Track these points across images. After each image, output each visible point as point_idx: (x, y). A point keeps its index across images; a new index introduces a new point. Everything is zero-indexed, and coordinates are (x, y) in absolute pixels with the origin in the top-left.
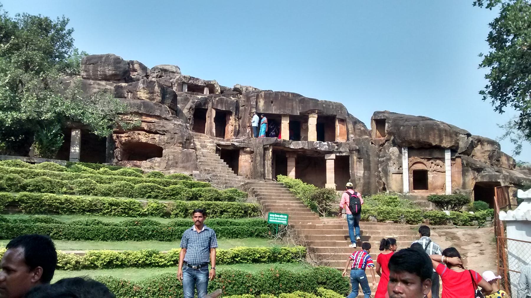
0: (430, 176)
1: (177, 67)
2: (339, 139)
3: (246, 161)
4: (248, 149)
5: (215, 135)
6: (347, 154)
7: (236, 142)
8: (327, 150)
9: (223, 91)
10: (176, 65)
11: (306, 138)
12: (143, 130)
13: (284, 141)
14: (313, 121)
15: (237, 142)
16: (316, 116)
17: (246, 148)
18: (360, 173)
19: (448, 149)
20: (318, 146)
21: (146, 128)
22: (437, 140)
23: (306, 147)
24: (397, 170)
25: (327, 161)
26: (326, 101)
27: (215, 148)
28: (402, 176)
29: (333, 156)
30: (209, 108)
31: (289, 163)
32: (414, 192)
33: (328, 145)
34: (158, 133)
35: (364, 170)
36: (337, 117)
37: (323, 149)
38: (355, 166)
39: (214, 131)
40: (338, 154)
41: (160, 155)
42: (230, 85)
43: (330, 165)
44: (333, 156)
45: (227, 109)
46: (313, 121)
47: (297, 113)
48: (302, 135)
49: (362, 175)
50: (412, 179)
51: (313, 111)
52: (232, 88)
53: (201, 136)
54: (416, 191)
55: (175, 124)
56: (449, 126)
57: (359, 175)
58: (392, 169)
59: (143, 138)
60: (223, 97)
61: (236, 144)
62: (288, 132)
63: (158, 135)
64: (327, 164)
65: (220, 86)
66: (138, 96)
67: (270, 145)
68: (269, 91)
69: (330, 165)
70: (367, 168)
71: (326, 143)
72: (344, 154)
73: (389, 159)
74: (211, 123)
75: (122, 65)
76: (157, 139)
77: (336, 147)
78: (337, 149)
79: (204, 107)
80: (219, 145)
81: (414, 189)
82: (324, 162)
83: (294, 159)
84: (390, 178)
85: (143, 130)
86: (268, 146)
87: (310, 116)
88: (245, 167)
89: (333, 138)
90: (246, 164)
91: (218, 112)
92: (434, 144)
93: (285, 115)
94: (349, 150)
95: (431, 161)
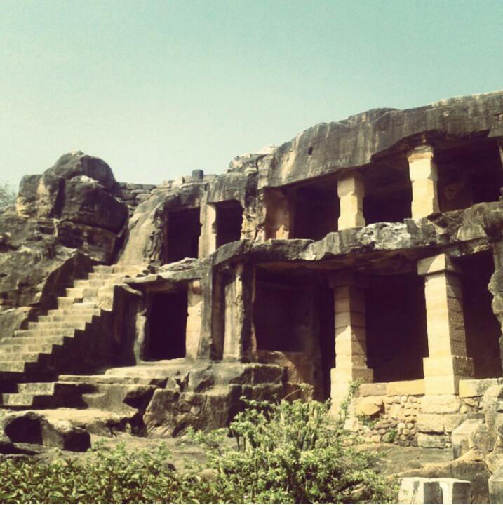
4: (196, 284)
6: (484, 247)
8: (409, 245)
15: (172, 269)
20: (373, 238)
23: (336, 250)
29: (439, 262)
30: (203, 205)
37: (392, 245)
40: (457, 253)
51: (412, 143)
74: (206, 237)
77: (440, 231)
78: (446, 236)
79: (190, 207)
91: (219, 207)
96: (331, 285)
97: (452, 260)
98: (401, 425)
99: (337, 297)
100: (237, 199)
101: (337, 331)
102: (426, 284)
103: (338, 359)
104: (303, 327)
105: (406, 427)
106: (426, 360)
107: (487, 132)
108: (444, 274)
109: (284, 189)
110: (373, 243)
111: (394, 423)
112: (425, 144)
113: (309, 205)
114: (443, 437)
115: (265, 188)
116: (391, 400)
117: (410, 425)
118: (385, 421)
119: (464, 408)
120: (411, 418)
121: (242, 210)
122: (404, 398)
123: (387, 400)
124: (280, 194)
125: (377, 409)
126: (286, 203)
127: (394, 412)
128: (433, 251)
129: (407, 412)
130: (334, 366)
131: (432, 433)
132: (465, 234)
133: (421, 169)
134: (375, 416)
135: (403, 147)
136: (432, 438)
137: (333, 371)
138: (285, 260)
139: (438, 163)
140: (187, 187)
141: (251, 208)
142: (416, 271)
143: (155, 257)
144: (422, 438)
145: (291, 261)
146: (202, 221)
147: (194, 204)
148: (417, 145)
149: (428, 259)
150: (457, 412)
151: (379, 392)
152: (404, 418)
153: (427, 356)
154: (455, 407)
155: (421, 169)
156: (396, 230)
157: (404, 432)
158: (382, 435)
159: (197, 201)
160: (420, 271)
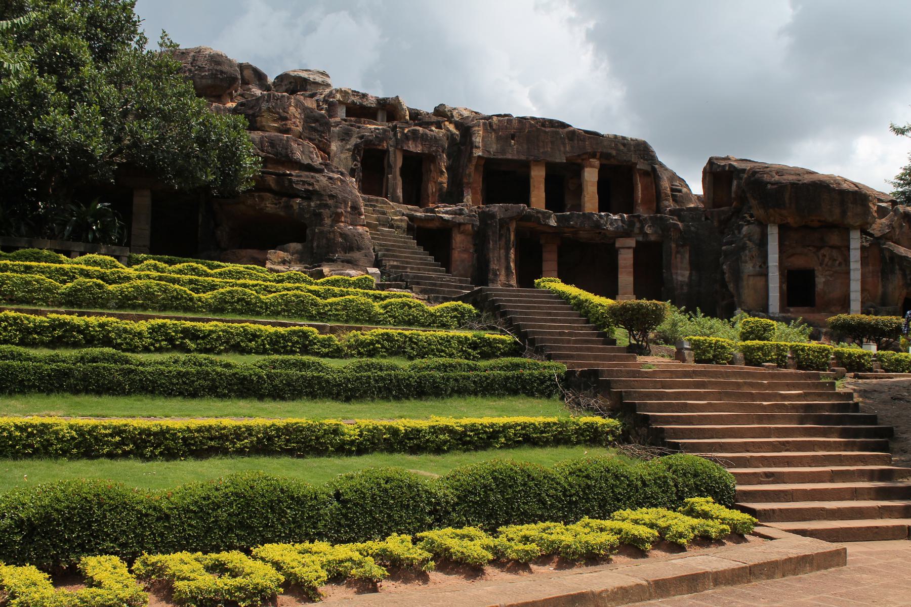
0: (820, 280)
1: (323, 74)
2: (642, 211)
3: (465, 251)
5: (401, 200)
7: (445, 212)
9: (415, 115)
10: (321, 70)
11: (579, 206)
12: (270, 190)
13: (538, 212)
14: (591, 176)
15: (446, 213)
16: (596, 162)
18: (683, 276)
19: (855, 228)
21: (273, 185)
22: (837, 211)
24: (758, 269)
25: (622, 251)
26: (616, 137)
27: (404, 225)
28: (767, 281)
29: (632, 242)
31: (546, 256)
32: (789, 311)
33: (623, 220)
34: (298, 197)
35: (691, 270)
36: (638, 167)
40: (640, 239)
41: (300, 239)
42: (427, 107)
43: (626, 259)
44: (632, 242)
46: (591, 176)
47: (561, 159)
48: (569, 203)
49: (686, 280)
50: (785, 287)
52: (431, 111)
53: (377, 201)
54: (792, 309)
55: (330, 178)
56: (855, 185)
57: (680, 278)
58: (749, 268)
59: (270, 205)
60: (417, 128)
61: (446, 216)
62: (543, 195)
63: (298, 201)
64: (620, 257)
65: (410, 110)
66: (258, 125)
67: (511, 219)
68: (505, 115)
69: (626, 259)
70: (695, 266)
71: (616, 217)
73: (744, 248)
75: (226, 68)
76: (296, 207)
80: (412, 218)
81: (789, 306)
82: (613, 254)
84: (745, 283)
85: (270, 190)
89: (628, 206)
90: (465, 256)
92: (830, 220)
93: (537, 162)
95: (822, 251)
97: (637, 242)
108: (631, 251)
135: (584, 157)
139: (602, 171)
142: (614, 243)
160: (617, 245)
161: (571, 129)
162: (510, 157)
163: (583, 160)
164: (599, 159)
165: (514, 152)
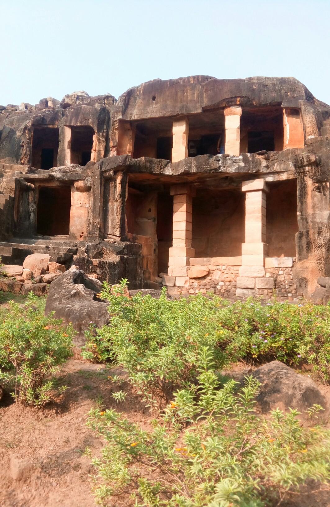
6: (291, 177)
8: (243, 171)
16: (239, 110)
17: (78, 181)
23: (194, 170)
25: (249, 196)
29: (259, 184)
36: (282, 105)
38: (309, 201)
39: (68, 162)
40: (270, 179)
45: (83, 124)
51: (230, 103)
72: (284, 177)
74: (63, 150)
78: (267, 167)
79: (51, 126)
82: (240, 198)
83: (184, 198)
86: (111, 172)
87: (226, 111)
88: (80, 217)
93: (177, 118)
94: (295, 166)
96: (172, 193)
97: (267, 184)
98: (221, 284)
99: (174, 202)
100: (91, 125)
101: (174, 223)
102: (247, 197)
103: (174, 242)
104: (146, 220)
105: (225, 284)
106: (244, 247)
107: (280, 104)
109: (131, 122)
110: (219, 167)
111: (216, 282)
112: (237, 105)
113: (151, 138)
114: (253, 291)
115: (120, 120)
116: (215, 268)
117: (227, 284)
118: (209, 281)
119: (268, 275)
120: (229, 279)
121: (93, 133)
122: (224, 267)
123: (211, 268)
124: (128, 126)
125: (206, 273)
126: (130, 133)
127: (216, 276)
128: (256, 176)
129: (226, 276)
130: (171, 246)
131: (247, 288)
132: (280, 167)
133: (232, 122)
134: (204, 278)
135: (224, 105)
136: (245, 291)
137: (170, 249)
138: (151, 173)
140: (49, 111)
141: (101, 134)
142: (241, 189)
143: (24, 161)
144: (239, 292)
145: (155, 174)
146: (60, 137)
147: (53, 124)
148: (232, 105)
149: (251, 181)
150: (263, 277)
151: (205, 263)
152: (223, 279)
153: (244, 242)
154: (263, 273)
155: (232, 122)
156: (236, 160)
157: (224, 288)
158: (207, 289)
159: (57, 123)
160: (244, 188)
161: (210, 80)
162: (149, 116)
163: (224, 108)
164: (241, 105)
165: (154, 111)
